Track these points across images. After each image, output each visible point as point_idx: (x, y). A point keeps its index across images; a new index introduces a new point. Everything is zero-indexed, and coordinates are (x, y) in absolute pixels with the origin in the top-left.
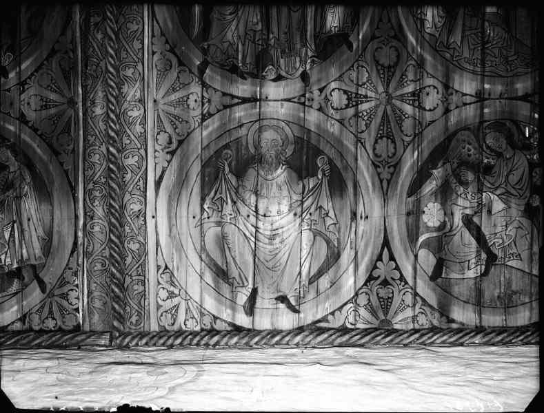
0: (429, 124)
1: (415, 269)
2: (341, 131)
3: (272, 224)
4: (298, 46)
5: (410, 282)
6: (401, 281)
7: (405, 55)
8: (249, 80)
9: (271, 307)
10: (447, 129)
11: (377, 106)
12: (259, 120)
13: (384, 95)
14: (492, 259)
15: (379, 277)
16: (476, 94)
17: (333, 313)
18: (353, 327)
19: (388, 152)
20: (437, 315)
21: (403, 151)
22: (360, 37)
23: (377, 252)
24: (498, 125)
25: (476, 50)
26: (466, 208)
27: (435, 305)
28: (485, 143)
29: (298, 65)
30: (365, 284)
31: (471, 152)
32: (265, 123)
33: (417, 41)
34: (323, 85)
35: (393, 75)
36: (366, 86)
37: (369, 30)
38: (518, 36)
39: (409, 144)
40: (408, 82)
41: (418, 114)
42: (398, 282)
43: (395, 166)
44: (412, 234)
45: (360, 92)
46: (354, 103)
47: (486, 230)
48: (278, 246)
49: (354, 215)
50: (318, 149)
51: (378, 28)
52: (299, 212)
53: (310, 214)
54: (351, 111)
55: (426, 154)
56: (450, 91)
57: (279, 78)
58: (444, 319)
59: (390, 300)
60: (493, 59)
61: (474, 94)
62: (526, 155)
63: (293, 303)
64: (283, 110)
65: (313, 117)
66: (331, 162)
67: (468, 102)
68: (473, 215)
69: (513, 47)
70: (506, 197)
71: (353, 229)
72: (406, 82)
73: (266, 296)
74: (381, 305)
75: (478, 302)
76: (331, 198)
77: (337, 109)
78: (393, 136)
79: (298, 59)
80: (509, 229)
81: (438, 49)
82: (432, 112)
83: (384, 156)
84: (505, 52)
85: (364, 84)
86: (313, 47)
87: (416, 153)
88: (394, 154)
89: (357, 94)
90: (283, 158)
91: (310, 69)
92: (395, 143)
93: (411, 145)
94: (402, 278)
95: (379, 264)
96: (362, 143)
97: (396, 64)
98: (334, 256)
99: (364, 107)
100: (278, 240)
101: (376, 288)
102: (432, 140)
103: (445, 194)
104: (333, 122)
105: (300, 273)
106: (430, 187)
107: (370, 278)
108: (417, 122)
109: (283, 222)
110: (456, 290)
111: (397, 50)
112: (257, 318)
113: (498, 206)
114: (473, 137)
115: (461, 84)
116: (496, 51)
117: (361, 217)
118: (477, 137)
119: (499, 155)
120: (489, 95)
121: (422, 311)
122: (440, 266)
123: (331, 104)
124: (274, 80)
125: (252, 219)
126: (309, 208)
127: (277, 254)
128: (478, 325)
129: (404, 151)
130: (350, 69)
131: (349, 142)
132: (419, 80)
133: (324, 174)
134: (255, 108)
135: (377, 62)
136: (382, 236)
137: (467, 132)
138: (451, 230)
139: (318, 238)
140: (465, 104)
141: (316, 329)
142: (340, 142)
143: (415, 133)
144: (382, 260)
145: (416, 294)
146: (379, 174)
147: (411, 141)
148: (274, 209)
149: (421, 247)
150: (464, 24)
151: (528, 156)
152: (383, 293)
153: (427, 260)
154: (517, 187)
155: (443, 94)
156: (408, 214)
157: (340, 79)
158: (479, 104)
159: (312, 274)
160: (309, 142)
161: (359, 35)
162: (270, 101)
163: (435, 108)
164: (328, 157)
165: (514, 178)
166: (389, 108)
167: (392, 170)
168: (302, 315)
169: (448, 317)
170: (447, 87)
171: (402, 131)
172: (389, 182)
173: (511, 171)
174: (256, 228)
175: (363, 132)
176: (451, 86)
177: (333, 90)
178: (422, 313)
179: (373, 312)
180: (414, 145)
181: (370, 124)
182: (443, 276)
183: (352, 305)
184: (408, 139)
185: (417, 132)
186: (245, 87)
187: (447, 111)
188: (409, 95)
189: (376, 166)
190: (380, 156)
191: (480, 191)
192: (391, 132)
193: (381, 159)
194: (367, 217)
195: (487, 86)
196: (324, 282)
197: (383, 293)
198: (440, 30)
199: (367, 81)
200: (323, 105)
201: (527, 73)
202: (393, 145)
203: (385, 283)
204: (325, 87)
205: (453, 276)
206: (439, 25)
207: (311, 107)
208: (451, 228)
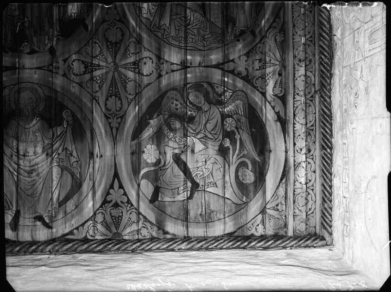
0: (147, 86)
1: (138, 195)
2: (80, 92)
3: (30, 162)
4: (47, 28)
5: (134, 203)
6: (128, 204)
7: (128, 34)
8: (10, 54)
9: (31, 224)
10: (160, 90)
11: (107, 73)
12: (18, 83)
13: (112, 64)
14: (195, 185)
15: (111, 201)
16: (181, 63)
17: (77, 228)
18: (92, 238)
20: (155, 228)
21: (127, 106)
22: (94, 21)
23: (110, 182)
24: (198, 86)
25: (180, 30)
26: (176, 148)
27: (153, 220)
28: (189, 100)
29: (47, 42)
30: (101, 206)
31: (178, 107)
32: (23, 85)
33: (137, 25)
34: (67, 57)
35: (119, 49)
36: (98, 58)
37: (100, 17)
38: (212, 20)
39: (132, 101)
40: (131, 55)
41: (138, 78)
42: (126, 204)
43: (122, 117)
45: (94, 62)
46: (90, 71)
47: (190, 165)
48: (35, 178)
49: (92, 154)
50: (64, 105)
51: (107, 13)
52: (49, 152)
53: (59, 154)
54: (87, 76)
55: (144, 108)
56: (162, 60)
57: (32, 52)
58: (161, 231)
59: (120, 218)
60: (194, 37)
61: (180, 64)
62: (218, 109)
63: (47, 221)
64: (36, 76)
65: (59, 81)
66: (73, 115)
67: (175, 69)
68: (180, 154)
69: (208, 28)
70: (204, 140)
71: (91, 165)
72: (129, 54)
73: (27, 216)
74: (114, 222)
75: (185, 219)
76: (74, 141)
77: (77, 75)
78: (120, 95)
79: (47, 37)
80: (207, 164)
81: (152, 29)
83: (113, 110)
84: (202, 32)
85: (97, 56)
86: (58, 28)
87: (137, 107)
88: (121, 108)
89: (92, 63)
90: (37, 112)
91: (56, 45)
92: (122, 101)
93: (133, 102)
94: (129, 202)
95: (111, 191)
96: (96, 100)
97: (122, 40)
98: (77, 186)
99: (97, 73)
100: (34, 174)
102: (150, 98)
103: (159, 138)
104: (74, 85)
105: (52, 199)
106: (148, 133)
107: (105, 202)
108: (138, 84)
109: (37, 160)
110: (169, 210)
111: (122, 30)
112: (20, 233)
113: (199, 146)
114: (179, 96)
115: (170, 55)
116: (195, 31)
117: (97, 156)
118: (182, 96)
120: (191, 64)
121: (144, 225)
122: (157, 192)
123: (73, 71)
124: (29, 54)
125: (15, 158)
126: (58, 149)
127: (34, 184)
128: (186, 235)
129: (128, 107)
130: (86, 45)
131: (86, 100)
132: (138, 53)
133: (68, 124)
134: (15, 74)
135: (107, 40)
137: (175, 92)
138: (164, 166)
139: (65, 172)
140: (173, 71)
141: (64, 240)
142: (81, 100)
143: (136, 93)
144: (113, 189)
145: (139, 213)
146: (110, 124)
148: (31, 151)
150: (171, 11)
152: (115, 212)
153: (147, 188)
154: (213, 132)
155: (157, 64)
156: (132, 154)
157: (78, 52)
159: (61, 199)
160: (56, 99)
161: (92, 19)
162: (27, 69)
163: (151, 74)
164: (71, 111)
165: (210, 126)
166: (116, 74)
167: (119, 120)
168: (54, 230)
169: (163, 230)
170: (159, 58)
171: (126, 91)
172: (117, 129)
173: (208, 121)
174: (18, 165)
175: (97, 92)
176: (162, 57)
177: (74, 60)
178: (144, 227)
179: (107, 227)
180: (135, 101)
181: (102, 86)
182: (160, 199)
183: (91, 222)
184: (131, 97)
185: (137, 92)
186: (7, 59)
189: (107, 118)
190: (110, 110)
191: (186, 136)
192: (118, 92)
193: (111, 112)
194: (101, 156)
195: (189, 57)
196: (70, 205)
197: (115, 212)
198: (153, 15)
199: (100, 54)
200: (67, 72)
201: (219, 47)
202: (119, 102)
203: (116, 205)
204: (69, 57)
205: (167, 199)
206: (153, 11)
207: (57, 73)
208: (165, 163)
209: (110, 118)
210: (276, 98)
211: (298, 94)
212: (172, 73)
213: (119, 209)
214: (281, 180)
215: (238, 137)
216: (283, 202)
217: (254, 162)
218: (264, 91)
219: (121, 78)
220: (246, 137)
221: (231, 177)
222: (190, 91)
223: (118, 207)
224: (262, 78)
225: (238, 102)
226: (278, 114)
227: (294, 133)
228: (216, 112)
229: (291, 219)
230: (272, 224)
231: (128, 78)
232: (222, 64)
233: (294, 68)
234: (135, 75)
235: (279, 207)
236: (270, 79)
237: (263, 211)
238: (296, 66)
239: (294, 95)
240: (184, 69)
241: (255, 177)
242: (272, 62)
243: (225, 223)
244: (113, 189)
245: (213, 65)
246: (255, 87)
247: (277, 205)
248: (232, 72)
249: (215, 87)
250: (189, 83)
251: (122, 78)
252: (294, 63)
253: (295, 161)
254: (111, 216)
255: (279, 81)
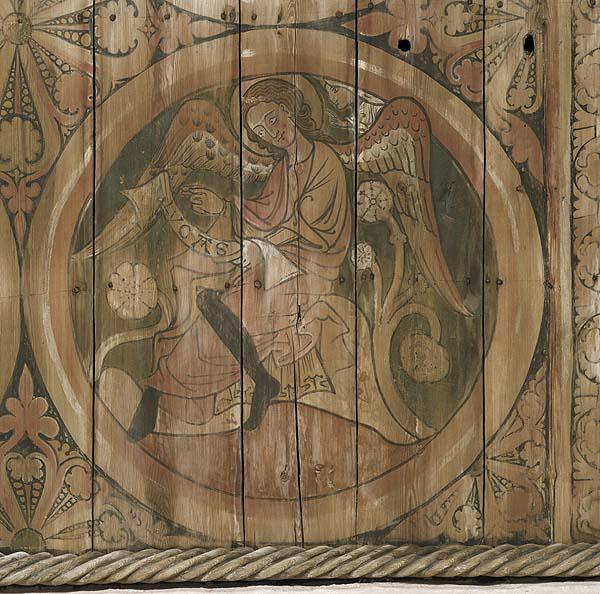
5: (83, 444)
6: (62, 442)
13: (13, 20)
14: (266, 388)
15: (11, 433)
16: (224, 16)
19: (24, 149)
20: (146, 517)
24: (275, 87)
26: (207, 275)
28: (248, 128)
31: (215, 149)
43: (41, 181)
44: (86, 332)
56: (164, 11)
59: (37, 486)
68: (221, 293)
74: (18, 497)
78: (35, 112)
80: (304, 322)
82: (125, 58)
88: (39, 156)
93: (77, 134)
94: (63, 435)
101: (5, 460)
103: (156, 246)
106: (122, 228)
110: (184, 466)
113: (278, 270)
118: (227, 116)
119: (280, 156)
120: (254, 18)
121: (109, 507)
122: (150, 401)
128: (239, 539)
129: (62, 149)
136: (17, 341)
144: (17, 396)
145: (95, 471)
147: (76, 126)
149: (106, 364)
151: (343, 157)
152: (18, 467)
153: (121, 395)
154: (320, 226)
156: (75, 291)
158: (230, 38)
163: (128, 53)
165: (312, 208)
166: (24, 50)
167: (35, 188)
169: (170, 523)
171: (56, 103)
172: (28, 217)
173: (304, 192)
178: (111, 513)
182: (158, 428)
187: (158, 56)
188: (71, 20)
192: (32, 104)
208: (174, 320)
209: (6, 184)
210: (517, 120)
211: (584, 108)
212: (196, 48)
213: (33, 458)
214: (533, 370)
215: (397, 239)
216: (539, 439)
217: (447, 313)
218: (479, 100)
219: (38, 64)
220: (422, 237)
221: (375, 363)
222: (251, 100)
223: (31, 451)
224: (473, 60)
225: (399, 133)
226: (522, 169)
227: (573, 228)
228: (327, 164)
229: (562, 489)
230: (504, 504)
231: (59, 62)
232: (349, 17)
233: (574, 27)
234: (83, 52)
235: (526, 454)
236: (498, 60)
237: (477, 466)
238: (581, 20)
239: (574, 110)
240: (233, 32)
241: (453, 359)
242: (504, 8)
243: (358, 503)
244: (17, 396)
245: (324, 20)
246: (450, 88)
247: (521, 448)
248: (380, 42)
249: (328, 88)
250: (249, 78)
251: (43, 62)
252: (573, 13)
253: (575, 313)
254: (10, 478)
255: (527, 69)
